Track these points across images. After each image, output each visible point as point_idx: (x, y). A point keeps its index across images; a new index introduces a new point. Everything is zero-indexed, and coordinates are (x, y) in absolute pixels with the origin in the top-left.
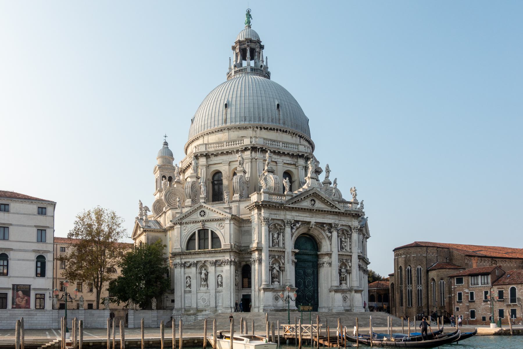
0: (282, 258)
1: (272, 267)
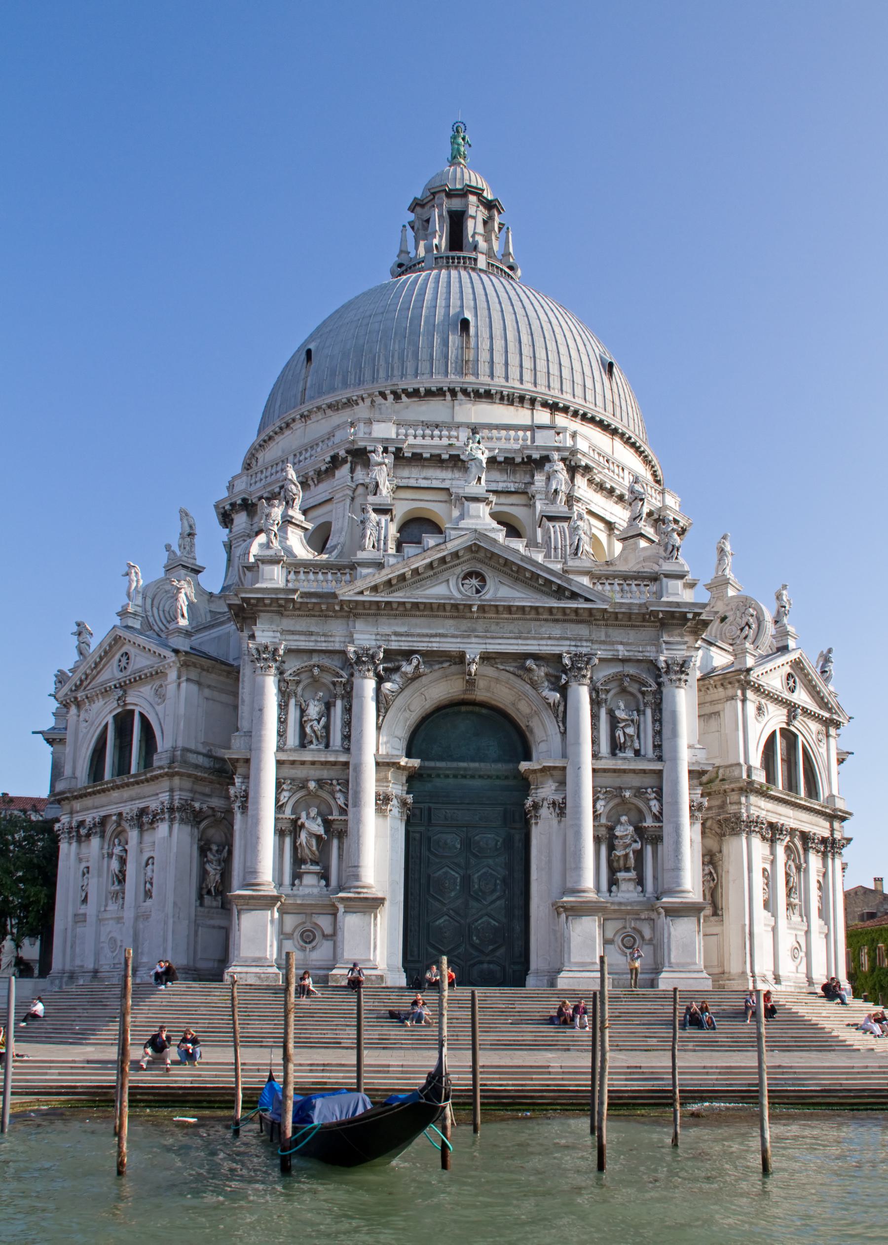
0: (338, 787)
1: (294, 822)
